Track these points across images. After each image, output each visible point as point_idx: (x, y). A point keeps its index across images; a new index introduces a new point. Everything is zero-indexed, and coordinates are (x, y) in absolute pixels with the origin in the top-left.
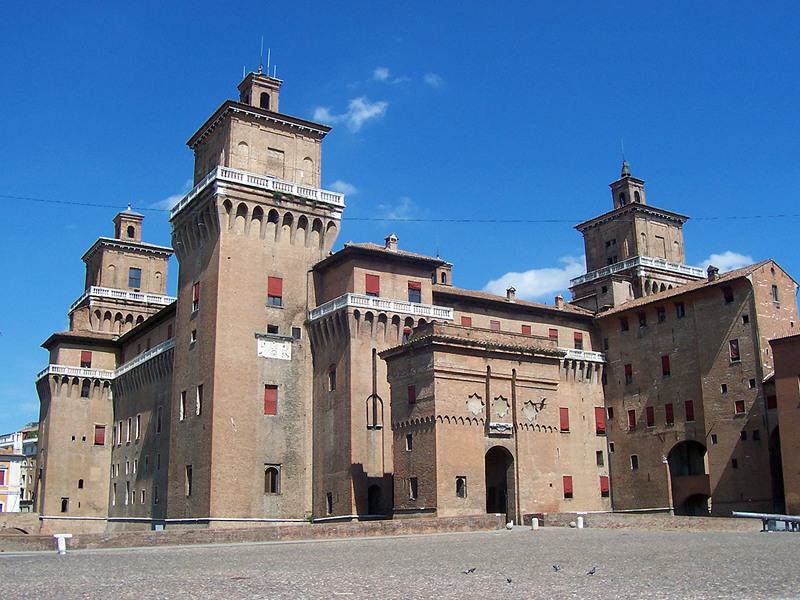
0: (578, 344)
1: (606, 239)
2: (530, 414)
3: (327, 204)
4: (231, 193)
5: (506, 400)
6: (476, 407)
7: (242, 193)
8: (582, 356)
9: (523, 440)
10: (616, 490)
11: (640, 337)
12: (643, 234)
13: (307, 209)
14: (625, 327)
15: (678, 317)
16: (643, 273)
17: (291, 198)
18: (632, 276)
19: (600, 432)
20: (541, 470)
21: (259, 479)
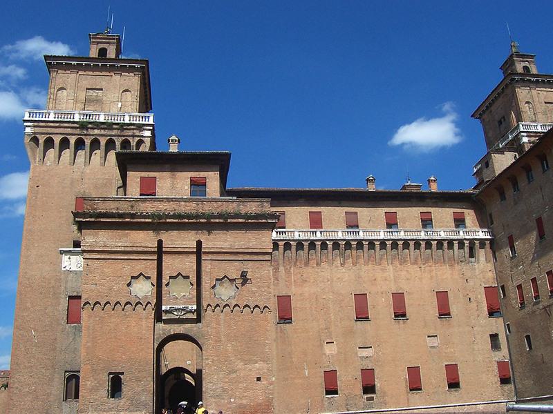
0: (459, 222)
1: (497, 118)
2: (226, 292)
3: (134, 124)
4: (38, 130)
5: (188, 277)
6: (143, 289)
7: (48, 129)
8: (462, 235)
9: (214, 325)
10: (517, 374)
11: (516, 203)
12: (527, 102)
13: (114, 132)
14: (503, 196)
15: (544, 171)
16: (525, 140)
17: (98, 125)
18: (515, 145)
19: (491, 314)
20: (242, 360)
21: (58, 386)
